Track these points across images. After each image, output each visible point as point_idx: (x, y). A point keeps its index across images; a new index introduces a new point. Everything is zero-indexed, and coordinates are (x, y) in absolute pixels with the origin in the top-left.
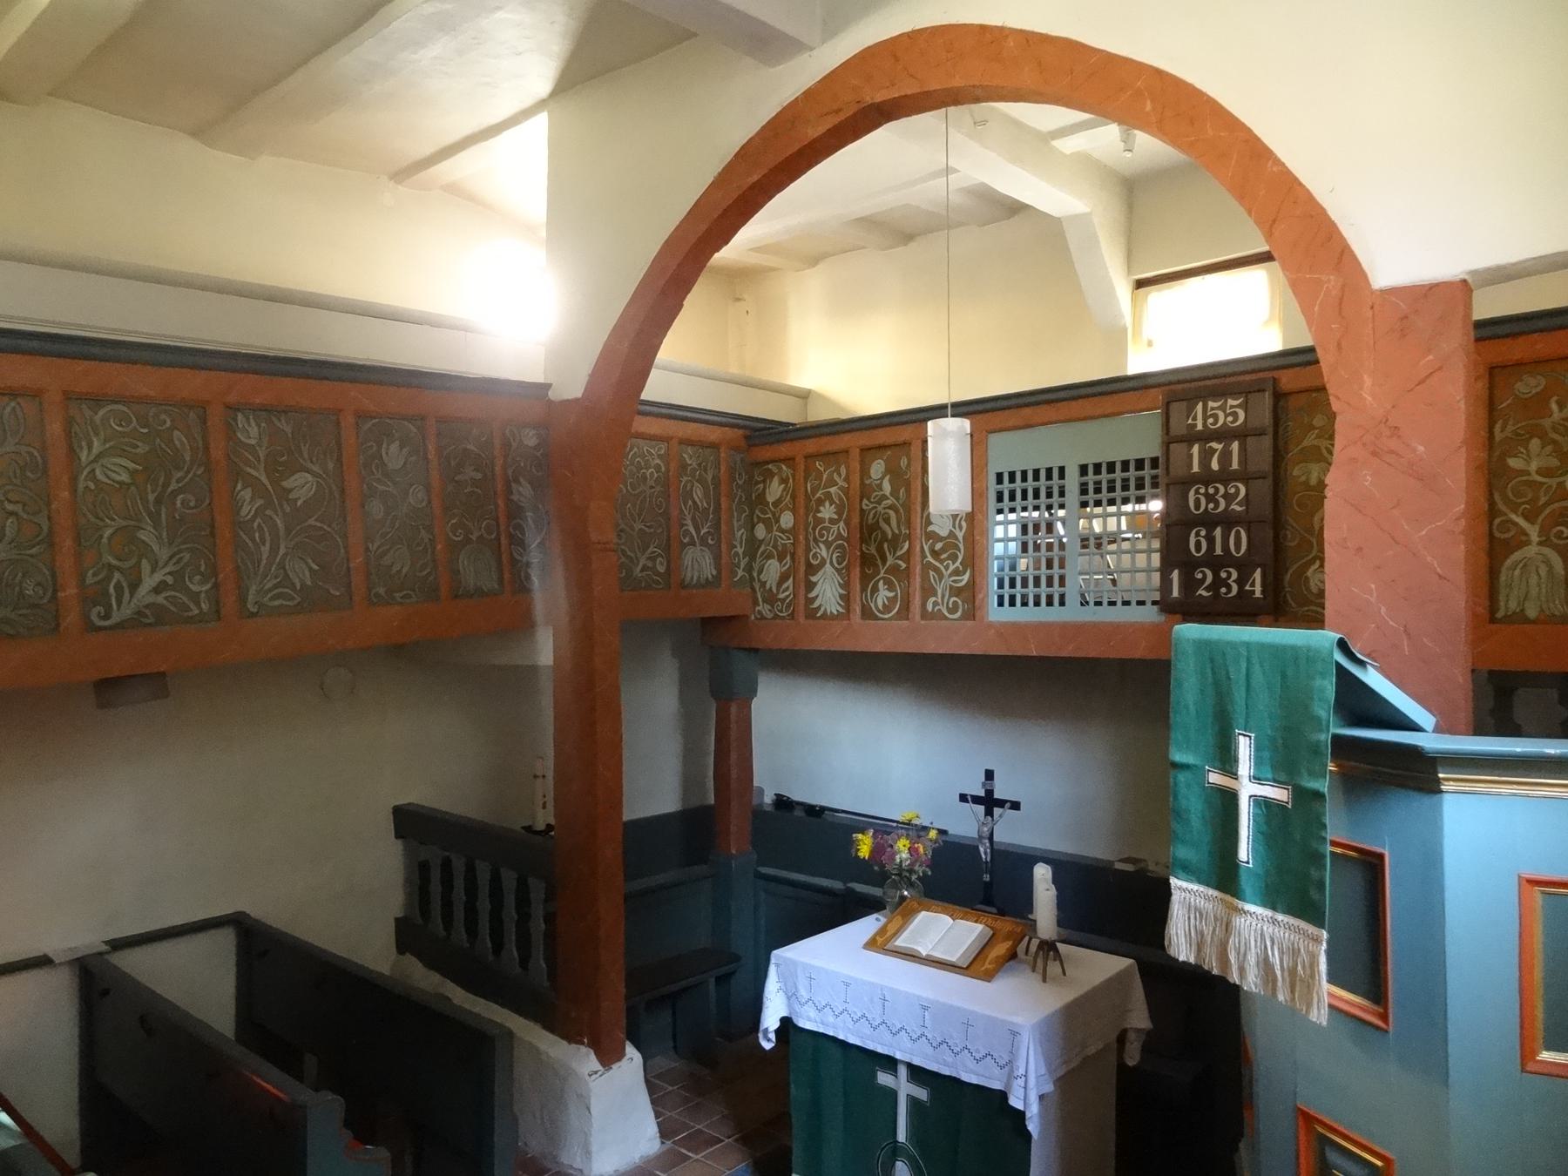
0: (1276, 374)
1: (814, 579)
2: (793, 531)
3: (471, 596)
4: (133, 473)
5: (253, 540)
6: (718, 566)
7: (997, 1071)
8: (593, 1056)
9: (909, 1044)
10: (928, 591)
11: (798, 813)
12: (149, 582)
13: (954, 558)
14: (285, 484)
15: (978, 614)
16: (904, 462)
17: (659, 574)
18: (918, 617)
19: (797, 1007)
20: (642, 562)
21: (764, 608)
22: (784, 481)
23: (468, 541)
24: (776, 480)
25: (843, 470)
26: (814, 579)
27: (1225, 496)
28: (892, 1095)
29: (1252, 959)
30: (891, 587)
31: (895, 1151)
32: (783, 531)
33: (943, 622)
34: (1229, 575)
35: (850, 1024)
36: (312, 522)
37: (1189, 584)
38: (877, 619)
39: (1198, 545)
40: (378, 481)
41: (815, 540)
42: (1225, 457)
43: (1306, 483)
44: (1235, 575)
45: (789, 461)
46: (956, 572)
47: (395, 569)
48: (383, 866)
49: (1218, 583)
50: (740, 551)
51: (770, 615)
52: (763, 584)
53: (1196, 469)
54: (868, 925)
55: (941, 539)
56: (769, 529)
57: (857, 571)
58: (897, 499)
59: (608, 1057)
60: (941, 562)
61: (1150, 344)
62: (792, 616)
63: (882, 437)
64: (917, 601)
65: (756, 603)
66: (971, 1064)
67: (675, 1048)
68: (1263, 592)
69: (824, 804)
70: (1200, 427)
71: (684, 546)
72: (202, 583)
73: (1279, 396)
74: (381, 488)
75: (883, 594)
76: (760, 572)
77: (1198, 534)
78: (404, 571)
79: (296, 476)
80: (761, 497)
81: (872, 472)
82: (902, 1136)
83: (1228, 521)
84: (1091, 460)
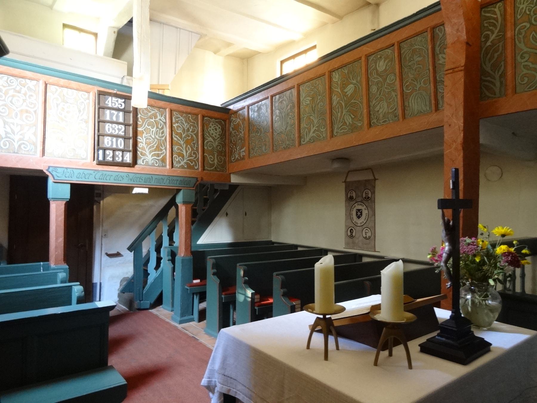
5: (336, 112)
12: (312, 131)
14: (345, 91)
40: (374, 78)
72: (324, 128)
74: (376, 80)
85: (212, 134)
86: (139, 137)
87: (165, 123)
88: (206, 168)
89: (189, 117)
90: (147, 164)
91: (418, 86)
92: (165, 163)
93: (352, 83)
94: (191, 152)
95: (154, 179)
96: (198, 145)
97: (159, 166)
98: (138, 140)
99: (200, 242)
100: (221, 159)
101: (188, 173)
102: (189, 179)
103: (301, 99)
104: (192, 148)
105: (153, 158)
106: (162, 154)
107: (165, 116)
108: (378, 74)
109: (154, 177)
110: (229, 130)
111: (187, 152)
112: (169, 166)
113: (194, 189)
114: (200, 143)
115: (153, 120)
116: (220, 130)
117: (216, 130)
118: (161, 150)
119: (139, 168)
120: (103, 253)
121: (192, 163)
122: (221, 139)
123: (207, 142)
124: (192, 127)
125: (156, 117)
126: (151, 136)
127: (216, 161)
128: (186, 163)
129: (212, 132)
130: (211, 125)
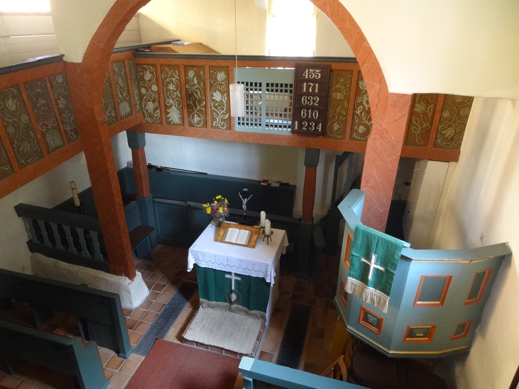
0: (331, 64)
1: (169, 111)
2: (158, 92)
3: (55, 150)
6: (131, 107)
7: (262, 273)
8: (127, 278)
9: (236, 269)
10: (214, 119)
11: (154, 170)
13: (223, 109)
15: (232, 129)
16: (202, 73)
17: (113, 117)
18: (210, 128)
19: (199, 262)
20: (107, 114)
21: (149, 120)
22: (151, 73)
23: (48, 130)
24: (148, 73)
25: (177, 72)
26: (169, 111)
27: (313, 100)
28: (231, 280)
29: (369, 298)
30: (199, 117)
31: (231, 291)
32: (154, 92)
33: (220, 130)
34: (312, 124)
35: (217, 265)
37: (300, 126)
38: (194, 126)
39: (304, 114)
40: (9, 118)
41: (168, 97)
42: (314, 88)
43: (336, 99)
44: (314, 124)
45: (154, 66)
46: (223, 114)
48: (18, 230)
49: (309, 126)
50: (137, 98)
51: (151, 122)
52: (147, 111)
53: (305, 91)
54: (210, 231)
55: (217, 102)
56: (147, 91)
57: (186, 111)
58: (200, 86)
59: (131, 276)
60: (218, 110)
61: (274, 16)
62: (161, 123)
63: (193, 62)
64: (209, 123)
65: (145, 117)
66: (255, 273)
67: (137, 256)
68: (321, 130)
69: (164, 166)
70: (307, 77)
71: (119, 103)
73: (331, 70)
74: (11, 120)
75: (196, 119)
76: (145, 106)
77: (304, 111)
80: (142, 78)
81: (189, 75)
82: (233, 288)
83: (313, 108)
84: (270, 82)
91: (50, 126)
108: (11, 114)
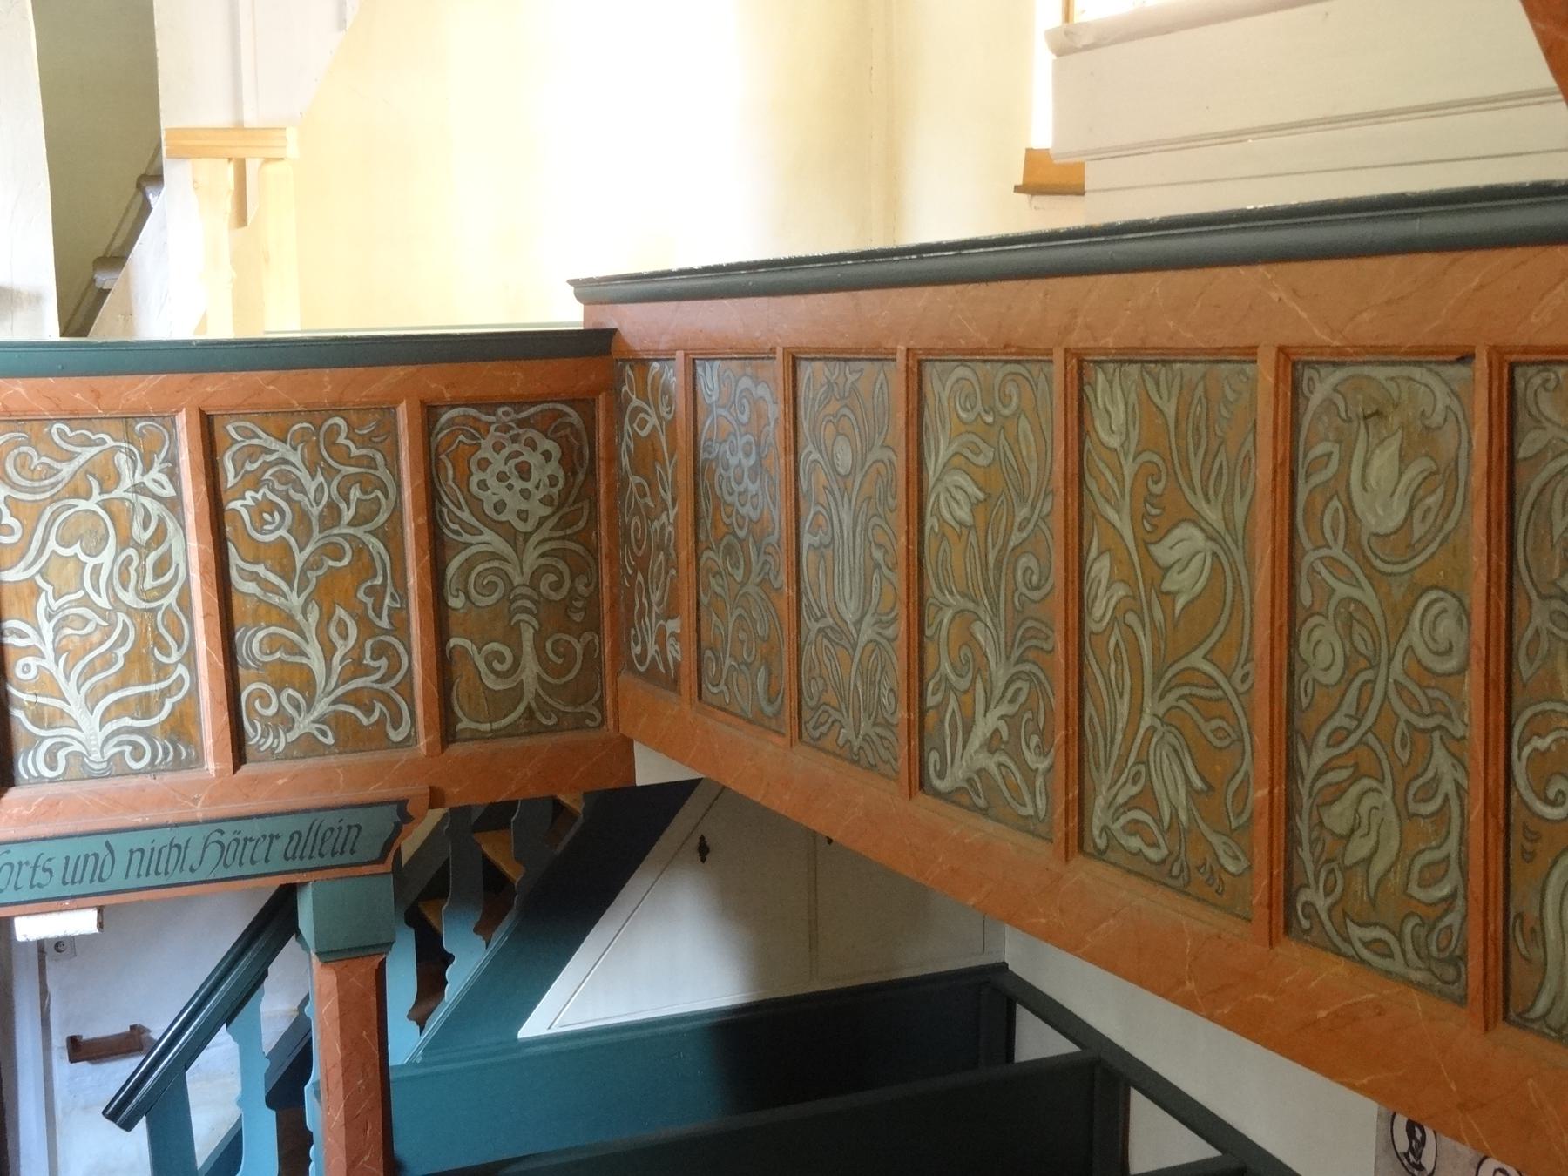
4: (975, 505)
36: (1196, 659)
47: (1359, 848)
72: (1042, 751)
74: (1343, 590)
78: (1378, 867)
79: (1177, 533)
85: (500, 506)
86: (10, 624)
87: (174, 505)
88: (464, 724)
89: (334, 430)
90: (79, 770)
92: (194, 743)
93: (1196, 520)
94: (360, 645)
95: (122, 858)
96: (404, 597)
97: (152, 769)
98: (9, 640)
99: (539, 1024)
100: (568, 655)
101: (342, 780)
102: (351, 818)
103: (932, 468)
104: (362, 621)
105: (111, 727)
106: (165, 693)
107: (173, 460)
108: (1353, 543)
109: (121, 844)
110: (613, 459)
111: (328, 650)
112: (216, 759)
113: (387, 866)
114: (412, 580)
115: (90, 505)
116: (554, 467)
117: (524, 472)
118: (163, 671)
119: (28, 803)
120: (59, 1041)
121: (369, 711)
122: (564, 523)
123: (469, 564)
124: (355, 493)
125: (109, 478)
126: (86, 602)
127: (530, 669)
128: (336, 721)
129: (497, 491)
130: (486, 452)
